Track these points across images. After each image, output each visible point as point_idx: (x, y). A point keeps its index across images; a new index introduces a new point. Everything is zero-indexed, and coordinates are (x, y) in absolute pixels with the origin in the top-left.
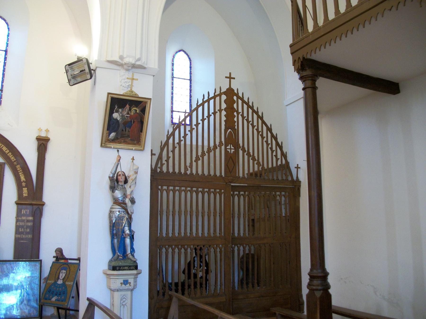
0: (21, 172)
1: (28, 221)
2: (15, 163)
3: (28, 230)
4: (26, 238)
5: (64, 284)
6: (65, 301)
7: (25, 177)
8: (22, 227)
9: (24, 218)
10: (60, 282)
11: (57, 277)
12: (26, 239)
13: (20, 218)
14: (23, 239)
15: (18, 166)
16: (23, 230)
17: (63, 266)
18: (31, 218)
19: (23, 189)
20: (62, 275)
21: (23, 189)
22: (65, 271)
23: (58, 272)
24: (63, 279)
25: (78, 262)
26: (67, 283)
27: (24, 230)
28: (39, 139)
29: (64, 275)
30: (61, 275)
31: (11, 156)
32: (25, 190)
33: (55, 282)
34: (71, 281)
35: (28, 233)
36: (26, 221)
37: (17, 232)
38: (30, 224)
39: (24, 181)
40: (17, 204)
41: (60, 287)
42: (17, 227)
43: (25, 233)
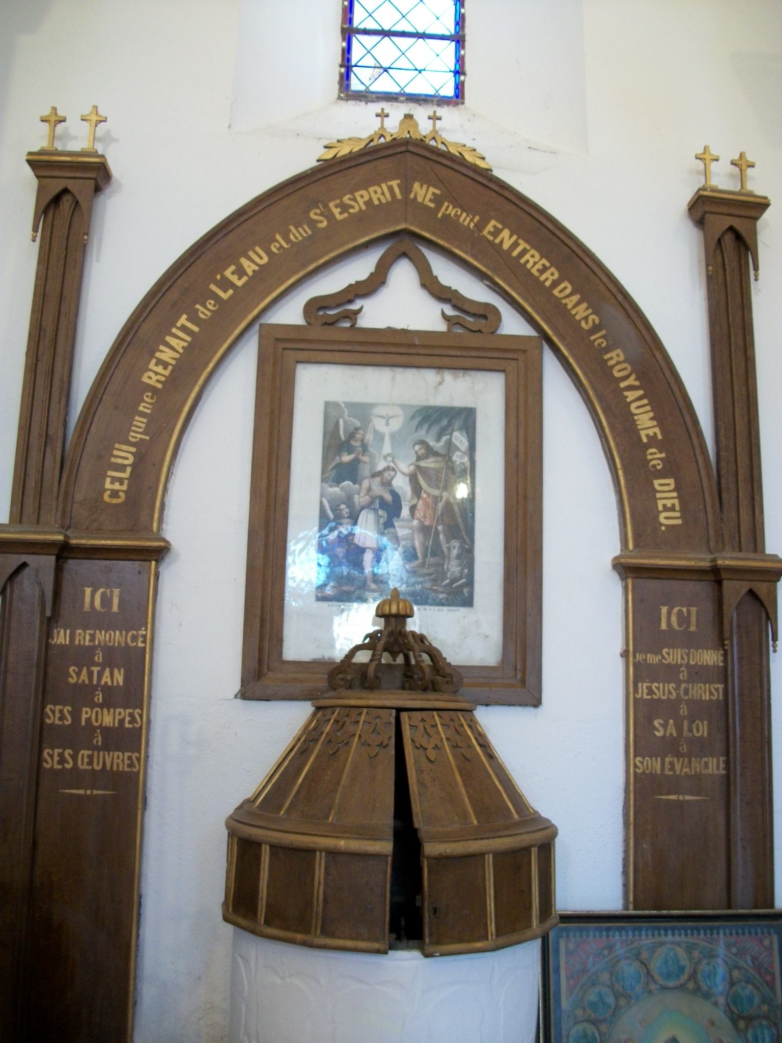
0: (631, 388)
1: (698, 674)
2: (597, 339)
3: (702, 729)
4: (698, 777)
7: (659, 418)
8: (668, 708)
9: (673, 656)
12: (696, 782)
13: (653, 659)
15: (615, 357)
16: (672, 730)
18: (710, 657)
19: (656, 483)
21: (656, 483)
28: (705, 208)
31: (571, 302)
32: (665, 491)
35: (700, 748)
36: (683, 675)
38: (710, 692)
39: (652, 439)
40: (626, 569)
42: (642, 716)
43: (684, 749)
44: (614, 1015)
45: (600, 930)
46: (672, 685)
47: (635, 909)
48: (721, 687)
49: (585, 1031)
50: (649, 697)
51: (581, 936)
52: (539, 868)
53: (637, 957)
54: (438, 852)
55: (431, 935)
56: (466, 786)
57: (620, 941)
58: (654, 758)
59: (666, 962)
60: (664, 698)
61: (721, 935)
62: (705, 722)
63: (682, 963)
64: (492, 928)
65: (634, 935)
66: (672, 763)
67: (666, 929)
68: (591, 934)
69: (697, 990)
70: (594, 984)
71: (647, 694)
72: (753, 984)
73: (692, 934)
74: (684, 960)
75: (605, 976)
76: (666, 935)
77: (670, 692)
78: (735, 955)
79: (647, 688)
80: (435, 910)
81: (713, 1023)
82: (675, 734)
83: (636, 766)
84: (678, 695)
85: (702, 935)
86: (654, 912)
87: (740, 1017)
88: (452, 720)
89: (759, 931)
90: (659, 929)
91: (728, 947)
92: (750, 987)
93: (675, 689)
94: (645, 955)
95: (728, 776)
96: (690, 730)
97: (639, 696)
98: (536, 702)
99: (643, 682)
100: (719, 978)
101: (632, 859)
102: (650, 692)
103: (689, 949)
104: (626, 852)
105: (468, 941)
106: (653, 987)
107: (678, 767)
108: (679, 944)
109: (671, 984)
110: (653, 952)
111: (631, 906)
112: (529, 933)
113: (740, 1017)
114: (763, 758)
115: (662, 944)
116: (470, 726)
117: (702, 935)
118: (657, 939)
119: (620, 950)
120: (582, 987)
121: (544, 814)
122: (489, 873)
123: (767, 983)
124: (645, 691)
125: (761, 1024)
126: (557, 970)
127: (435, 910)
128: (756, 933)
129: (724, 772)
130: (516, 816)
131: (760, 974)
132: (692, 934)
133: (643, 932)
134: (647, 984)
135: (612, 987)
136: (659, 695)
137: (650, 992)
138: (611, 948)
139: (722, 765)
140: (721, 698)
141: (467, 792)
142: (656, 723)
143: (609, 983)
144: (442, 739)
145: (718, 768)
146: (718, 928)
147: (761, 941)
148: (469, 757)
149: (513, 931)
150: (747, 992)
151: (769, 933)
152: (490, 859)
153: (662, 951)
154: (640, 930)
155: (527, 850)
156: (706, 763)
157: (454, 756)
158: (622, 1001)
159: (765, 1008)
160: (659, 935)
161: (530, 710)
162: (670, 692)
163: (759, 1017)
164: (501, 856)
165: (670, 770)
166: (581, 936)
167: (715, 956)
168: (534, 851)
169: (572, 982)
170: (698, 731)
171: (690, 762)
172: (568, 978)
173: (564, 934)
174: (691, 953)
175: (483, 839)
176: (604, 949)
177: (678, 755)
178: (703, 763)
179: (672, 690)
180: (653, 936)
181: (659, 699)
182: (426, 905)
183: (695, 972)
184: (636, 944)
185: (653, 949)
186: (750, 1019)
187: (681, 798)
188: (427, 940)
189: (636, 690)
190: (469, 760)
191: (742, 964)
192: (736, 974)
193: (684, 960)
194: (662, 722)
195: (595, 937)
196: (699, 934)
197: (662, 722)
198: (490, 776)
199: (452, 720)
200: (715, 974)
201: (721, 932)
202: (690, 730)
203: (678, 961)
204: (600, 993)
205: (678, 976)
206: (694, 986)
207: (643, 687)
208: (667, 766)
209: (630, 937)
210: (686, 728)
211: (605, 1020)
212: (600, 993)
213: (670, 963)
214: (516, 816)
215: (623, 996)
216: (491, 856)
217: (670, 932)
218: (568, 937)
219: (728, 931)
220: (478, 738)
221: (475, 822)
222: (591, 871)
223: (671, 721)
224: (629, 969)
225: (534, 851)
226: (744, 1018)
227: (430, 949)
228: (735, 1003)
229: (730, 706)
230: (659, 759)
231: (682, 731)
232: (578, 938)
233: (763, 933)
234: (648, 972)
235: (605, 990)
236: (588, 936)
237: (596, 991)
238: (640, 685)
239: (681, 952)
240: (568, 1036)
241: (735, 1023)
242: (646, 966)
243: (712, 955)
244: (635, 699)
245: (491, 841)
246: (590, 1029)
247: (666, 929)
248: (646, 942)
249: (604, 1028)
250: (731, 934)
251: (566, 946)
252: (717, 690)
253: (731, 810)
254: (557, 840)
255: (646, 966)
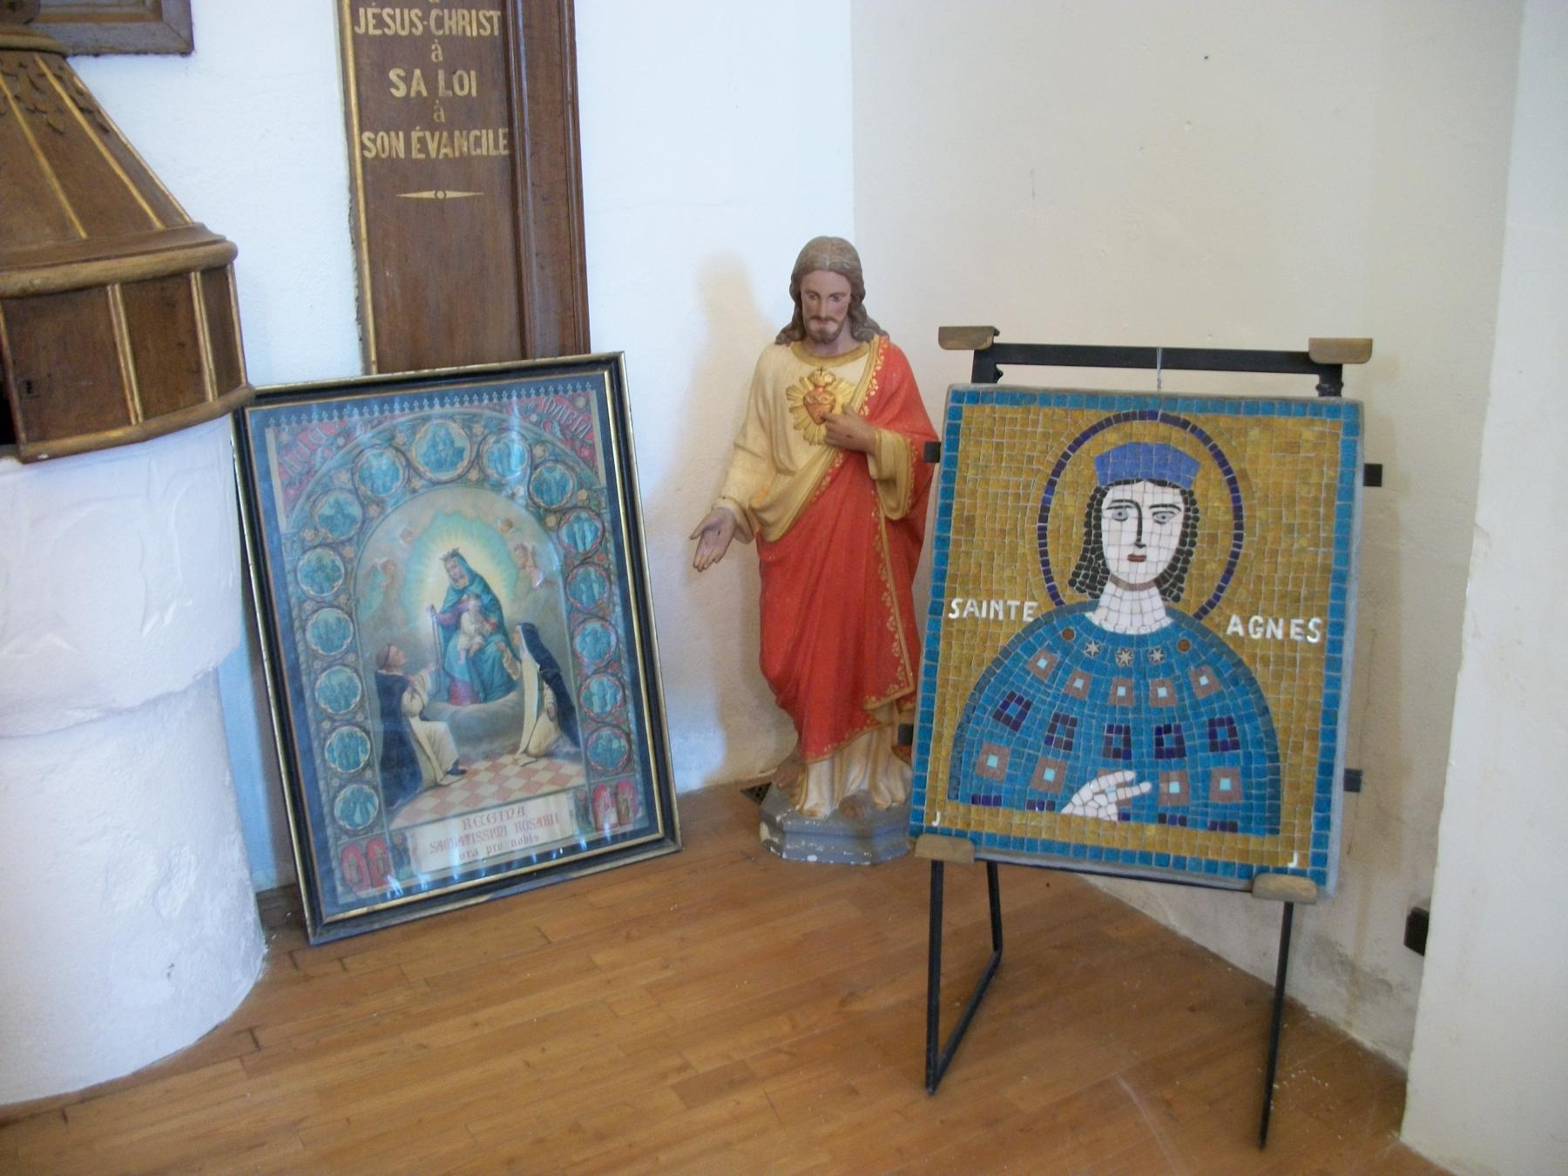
4: (466, 161)
5: (1193, 636)
6: (1272, 825)
8: (411, 51)
10: (1131, 611)
11: (1065, 559)
14: (428, 172)
16: (419, 86)
17: (1112, 438)
20: (1141, 533)
22: (1171, 496)
23: (1068, 504)
24: (1169, 582)
25: (1305, 385)
26: (1235, 626)
27: (430, 81)
29: (1163, 543)
30: (1116, 541)
33: (1064, 624)
34: (1290, 605)
35: (465, 115)
37: (369, 105)
41: (1141, 672)
43: (441, 116)
44: (361, 531)
45: (327, 407)
46: (416, 12)
47: (380, 372)
48: (495, 14)
49: (320, 560)
50: (378, 32)
51: (299, 422)
52: (206, 304)
53: (390, 441)
54: (19, 285)
55: (28, 428)
56: (59, 176)
57: (359, 421)
58: (392, 134)
59: (434, 445)
60: (404, 33)
61: (514, 398)
62: (473, 73)
63: (459, 444)
64: (135, 405)
65: (382, 411)
66: (422, 141)
67: (430, 398)
68: (315, 416)
69: (484, 480)
70: (327, 490)
71: (375, 27)
72: (564, 463)
73: (471, 401)
74: (461, 441)
75: (344, 477)
76: (431, 406)
77: (412, 24)
78: (537, 424)
79: (374, 16)
80: (29, 386)
81: (510, 524)
82: (425, 93)
83: (363, 147)
84: (427, 28)
85: (486, 401)
86: (411, 373)
87: (548, 511)
88: (21, 65)
89: (570, 387)
90: (419, 398)
91: (525, 414)
92: (560, 467)
93: (421, 19)
94: (400, 439)
95: (512, 157)
96: (449, 86)
97: (361, 31)
98: (186, 48)
99: (367, 5)
100: (514, 461)
101: (368, 296)
102: (380, 23)
103: (468, 422)
104: (360, 287)
105: (98, 430)
106: (417, 483)
107: (432, 147)
108: (452, 418)
109: (444, 476)
110: (414, 433)
111: (374, 368)
112: (201, 409)
113: (548, 511)
114: (565, 129)
115: (426, 419)
116: (59, 78)
117: (486, 401)
118: (418, 414)
119: (363, 436)
120: (309, 497)
121: (216, 227)
122: (118, 315)
123: (584, 459)
124: (372, 22)
125: (578, 518)
126: (267, 476)
127: (29, 386)
128: (566, 392)
129: (506, 152)
130: (158, 225)
131: (573, 448)
132: (471, 401)
133: (397, 406)
134: (409, 480)
135: (355, 491)
136: (393, 28)
137: (414, 491)
138: (348, 434)
139: (502, 142)
140: (496, 33)
141: (64, 187)
142: (393, 75)
143: (350, 486)
144: (5, 97)
145: (496, 146)
146: (509, 389)
147: (572, 401)
148: (61, 128)
149: (174, 408)
150: (557, 474)
151: (584, 389)
152: (115, 294)
153: (426, 432)
154: (391, 402)
155: (181, 275)
156: (478, 140)
157: (32, 125)
158: (373, 511)
159: (583, 494)
160: (421, 407)
161: (176, 60)
162: (412, 24)
163: (575, 507)
164: (134, 286)
165: (420, 151)
166: (299, 422)
167: (507, 429)
168: (196, 279)
169: (292, 492)
170: (462, 87)
171: (451, 137)
172: (286, 487)
173: (272, 421)
174: (470, 428)
175: (98, 259)
176: (339, 435)
177: (433, 127)
178: (472, 139)
179: (416, 20)
180: (412, 409)
181: (396, 35)
182: (11, 377)
183: (479, 456)
184: (386, 425)
185: (414, 428)
186: (562, 512)
187: (440, 195)
188: (22, 436)
189: (355, 21)
190: (61, 133)
191: (547, 436)
192: (538, 451)
193: (461, 441)
194: (402, 73)
195: (321, 420)
196: (481, 400)
197: (402, 73)
198: (104, 161)
199: (21, 65)
200: (509, 455)
201: (514, 393)
202: (449, 86)
203: (452, 442)
204: (337, 502)
205: (454, 465)
206: (478, 475)
207: (367, 15)
208: (415, 145)
209: (377, 414)
210: (441, 83)
211: (350, 540)
212: (337, 502)
213: (441, 447)
214: (158, 225)
215: (372, 502)
216: (117, 287)
217: (436, 401)
218: (278, 424)
219: (523, 392)
220: (77, 97)
221: (83, 235)
222: (302, 312)
223: (417, 72)
224: (380, 462)
225: (196, 279)
226: (555, 512)
227: (28, 449)
228: (539, 491)
229: (512, 46)
230: (401, 134)
231: (437, 88)
232: (294, 424)
233: (575, 390)
234: (409, 464)
235: (344, 497)
236: (310, 421)
237: (331, 500)
238: (362, 11)
239: (455, 429)
240: (295, 571)
241: (541, 520)
242: (404, 454)
243: (502, 429)
244: (355, 36)
245: (113, 263)
246: (329, 556)
247: (430, 398)
248: (403, 419)
249: (349, 551)
250: (528, 396)
251: (277, 437)
252: (490, 20)
253: (520, 211)
254: (236, 262)
255: (404, 454)
